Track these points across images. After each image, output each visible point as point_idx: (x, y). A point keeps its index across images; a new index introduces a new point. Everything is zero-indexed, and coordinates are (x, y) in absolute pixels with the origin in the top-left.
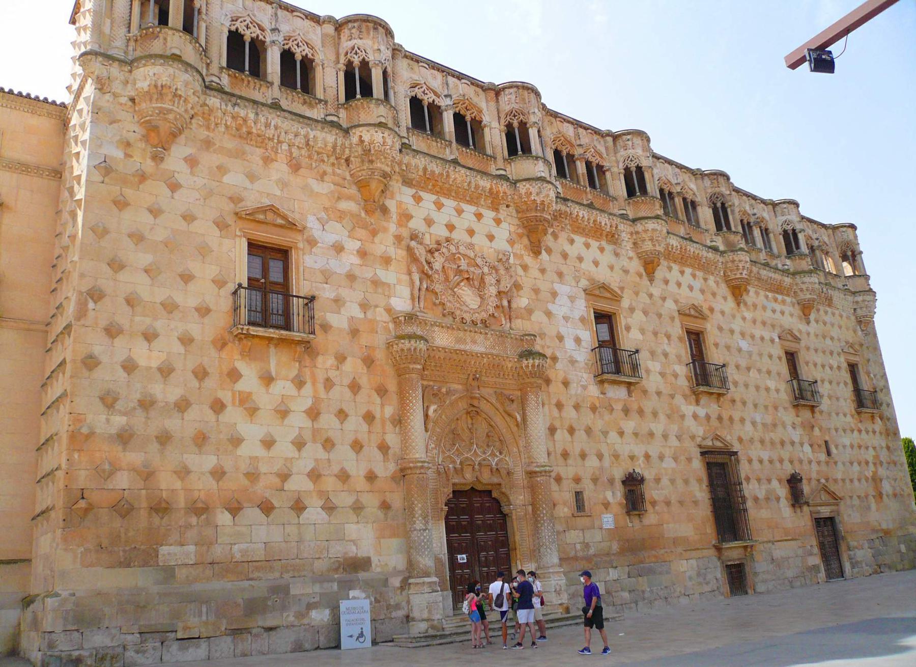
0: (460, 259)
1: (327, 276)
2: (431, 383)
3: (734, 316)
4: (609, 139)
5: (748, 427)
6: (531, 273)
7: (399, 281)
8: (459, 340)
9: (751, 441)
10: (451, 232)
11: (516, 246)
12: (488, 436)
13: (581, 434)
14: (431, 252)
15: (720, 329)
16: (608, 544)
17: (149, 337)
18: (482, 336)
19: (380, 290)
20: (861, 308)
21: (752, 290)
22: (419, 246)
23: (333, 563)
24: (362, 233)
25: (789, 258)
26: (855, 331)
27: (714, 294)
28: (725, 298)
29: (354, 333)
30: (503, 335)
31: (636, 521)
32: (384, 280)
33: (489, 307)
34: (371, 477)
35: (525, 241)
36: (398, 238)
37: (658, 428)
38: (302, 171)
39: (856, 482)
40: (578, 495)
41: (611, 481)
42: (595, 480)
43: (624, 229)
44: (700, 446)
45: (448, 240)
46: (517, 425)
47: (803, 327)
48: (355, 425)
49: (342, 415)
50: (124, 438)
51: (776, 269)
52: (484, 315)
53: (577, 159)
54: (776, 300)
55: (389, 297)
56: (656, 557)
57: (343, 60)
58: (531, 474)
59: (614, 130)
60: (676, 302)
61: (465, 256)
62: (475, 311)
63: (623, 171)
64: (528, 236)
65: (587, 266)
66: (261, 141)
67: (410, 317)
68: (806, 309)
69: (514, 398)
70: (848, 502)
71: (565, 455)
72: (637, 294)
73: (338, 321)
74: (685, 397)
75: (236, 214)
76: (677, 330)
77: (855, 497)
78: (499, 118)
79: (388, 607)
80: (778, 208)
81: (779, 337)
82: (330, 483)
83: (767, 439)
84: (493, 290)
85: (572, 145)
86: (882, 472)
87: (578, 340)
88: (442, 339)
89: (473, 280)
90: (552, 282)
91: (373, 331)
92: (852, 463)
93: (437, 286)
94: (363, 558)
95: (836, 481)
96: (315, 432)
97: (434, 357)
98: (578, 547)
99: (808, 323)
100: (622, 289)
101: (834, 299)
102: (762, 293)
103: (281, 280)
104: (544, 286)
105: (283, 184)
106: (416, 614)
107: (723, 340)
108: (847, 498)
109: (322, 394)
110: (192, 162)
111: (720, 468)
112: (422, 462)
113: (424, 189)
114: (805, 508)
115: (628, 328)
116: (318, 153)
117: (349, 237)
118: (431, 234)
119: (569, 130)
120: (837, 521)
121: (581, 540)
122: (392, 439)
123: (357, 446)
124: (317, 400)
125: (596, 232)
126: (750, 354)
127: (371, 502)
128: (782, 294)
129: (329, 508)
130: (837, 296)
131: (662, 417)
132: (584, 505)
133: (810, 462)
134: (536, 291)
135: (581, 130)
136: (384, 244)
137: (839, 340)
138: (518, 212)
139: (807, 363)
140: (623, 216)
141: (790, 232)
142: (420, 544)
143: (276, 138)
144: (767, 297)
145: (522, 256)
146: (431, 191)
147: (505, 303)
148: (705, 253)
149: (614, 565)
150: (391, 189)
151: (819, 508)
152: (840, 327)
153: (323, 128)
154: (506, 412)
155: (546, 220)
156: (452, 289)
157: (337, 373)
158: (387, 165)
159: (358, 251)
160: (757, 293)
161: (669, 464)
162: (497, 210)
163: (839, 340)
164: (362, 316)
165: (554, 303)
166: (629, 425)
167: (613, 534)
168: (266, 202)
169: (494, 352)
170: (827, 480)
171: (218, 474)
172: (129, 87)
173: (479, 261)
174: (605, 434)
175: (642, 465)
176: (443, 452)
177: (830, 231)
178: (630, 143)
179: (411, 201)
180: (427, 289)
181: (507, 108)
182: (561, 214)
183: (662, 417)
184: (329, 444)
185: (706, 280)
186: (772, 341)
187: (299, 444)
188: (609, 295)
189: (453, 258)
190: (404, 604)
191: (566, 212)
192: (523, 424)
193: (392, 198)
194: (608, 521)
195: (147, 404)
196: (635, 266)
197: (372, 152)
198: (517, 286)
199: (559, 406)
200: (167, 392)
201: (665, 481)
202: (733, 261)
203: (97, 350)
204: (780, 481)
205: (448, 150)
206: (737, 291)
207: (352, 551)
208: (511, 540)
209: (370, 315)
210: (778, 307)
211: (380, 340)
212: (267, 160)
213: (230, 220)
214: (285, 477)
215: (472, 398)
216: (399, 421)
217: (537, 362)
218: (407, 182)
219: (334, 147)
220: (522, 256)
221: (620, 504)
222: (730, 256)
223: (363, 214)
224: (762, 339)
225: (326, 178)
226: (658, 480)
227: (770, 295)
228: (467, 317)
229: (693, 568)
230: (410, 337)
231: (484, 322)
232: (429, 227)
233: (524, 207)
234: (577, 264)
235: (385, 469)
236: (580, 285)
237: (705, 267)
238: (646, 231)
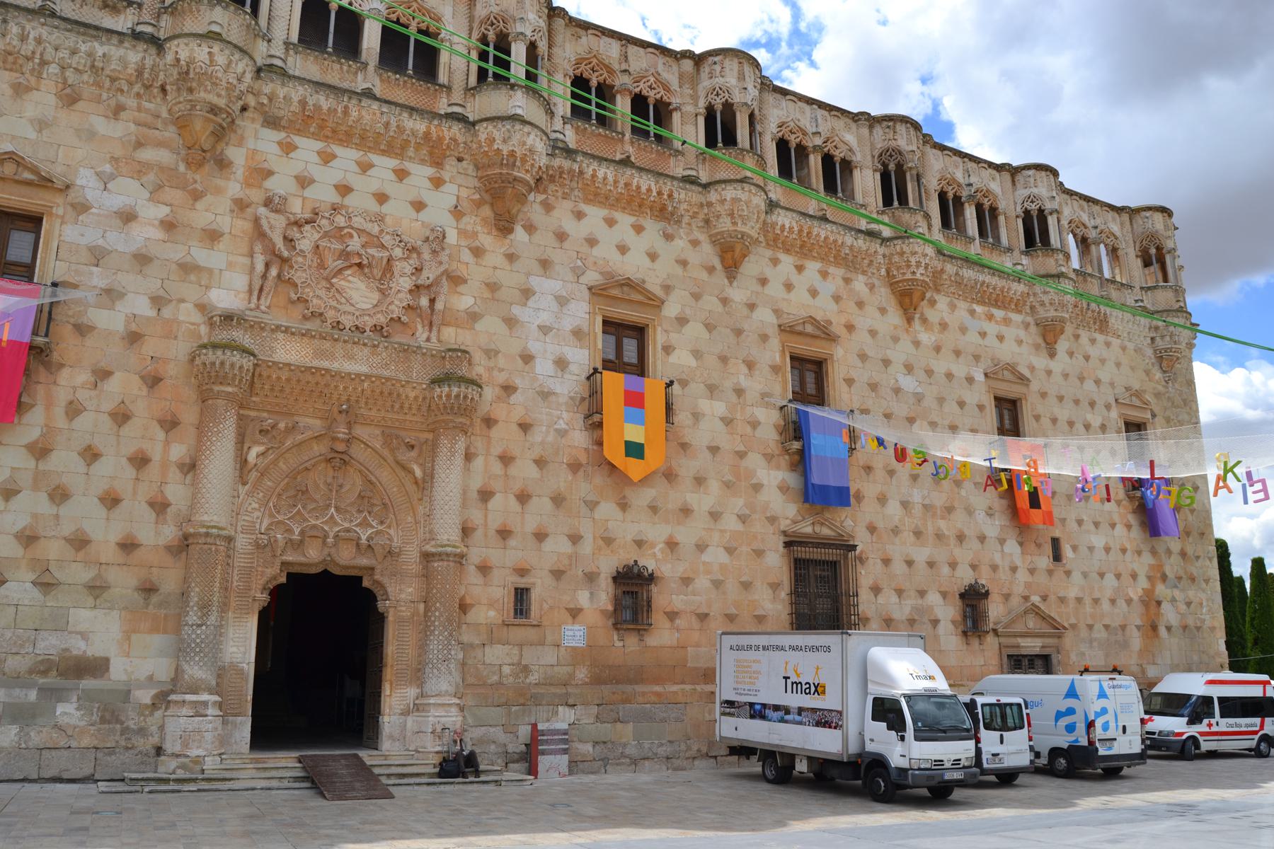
0: (351, 236)
1: (98, 256)
2: (265, 415)
3: (896, 339)
4: (688, 65)
5: (893, 508)
6: (486, 261)
7: (230, 265)
9: (896, 531)
10: (343, 196)
11: (466, 219)
12: (361, 497)
13: (541, 504)
14: (298, 224)
15: (863, 357)
16: (569, 669)
18: (366, 350)
19: (193, 277)
20: (1163, 337)
21: (942, 302)
22: (272, 215)
23: (42, 662)
24: (175, 195)
25: (1026, 253)
26: (1147, 372)
27: (860, 304)
28: (883, 311)
29: (134, 338)
30: (406, 350)
31: (632, 641)
32: (202, 264)
33: (392, 307)
34: (128, 546)
35: (487, 211)
36: (241, 205)
37: (702, 502)
38: (80, 105)
39: (1106, 605)
40: (521, 595)
41: (591, 578)
42: (558, 574)
43: (686, 197)
44: (785, 533)
45: (335, 208)
46: (416, 483)
47: (1041, 362)
48: (113, 469)
49: (91, 455)
51: (995, 271)
52: (382, 319)
53: (618, 92)
54: (990, 317)
55: (208, 287)
56: (658, 694)
58: (427, 557)
59: (698, 50)
60: (777, 312)
61: (361, 231)
62: (364, 313)
63: (703, 111)
64: (492, 205)
65: (605, 252)
68: (1049, 334)
69: (413, 442)
70: (1084, 633)
71: (504, 534)
72: (697, 297)
73: (110, 320)
74: (769, 457)
76: (774, 353)
77: (1098, 627)
78: (471, 30)
79: (125, 731)
80: (1019, 177)
81: (986, 375)
82: (53, 550)
83: (930, 530)
84: (406, 283)
85: (611, 71)
86: (1161, 590)
87: (561, 364)
88: (289, 352)
89: (370, 265)
90: (528, 274)
91: (170, 335)
92: (1102, 575)
93: (299, 273)
94: (96, 659)
95: (1062, 600)
97: (269, 377)
98: (506, 670)
99: (1052, 355)
100: (667, 288)
101: (1112, 320)
102: (962, 305)
103: (27, 259)
104: (509, 278)
105: (41, 125)
106: (169, 747)
107: (862, 375)
108: (1082, 626)
109: (61, 422)
112: (208, 527)
113: (299, 132)
114: (990, 639)
115: (668, 349)
116: (113, 80)
117: (150, 200)
118: (304, 199)
119: (612, 50)
120: (1054, 661)
121: (516, 660)
122: (176, 492)
123: (111, 501)
124: (49, 431)
125: (633, 202)
126: (919, 398)
127: (123, 581)
128: (1005, 308)
129: (46, 586)
130: (1117, 319)
131: (714, 486)
132: (528, 610)
133: (1014, 569)
135: (632, 49)
137: (1112, 384)
138: (477, 168)
139: (1037, 418)
140: (690, 181)
141: (1035, 214)
142: (189, 645)
143: (38, 56)
144: (972, 312)
145: (475, 234)
146: (315, 136)
147: (424, 302)
148: (849, 239)
149: (571, 701)
150: (239, 132)
151: (1019, 640)
152: (1118, 365)
153: (121, 42)
154: (398, 462)
155: (515, 179)
156: (327, 279)
157: (93, 393)
158: (219, 96)
159: (162, 222)
160: (953, 307)
161: (715, 555)
162: (438, 164)
163: (1112, 384)
164: (151, 313)
165: (525, 305)
168: (10, 148)
169: (386, 373)
170: (1044, 598)
173: (387, 240)
174: (592, 505)
175: (659, 555)
176: (271, 516)
177: (1126, 217)
178: (718, 68)
179: (275, 149)
180: (279, 276)
182: (561, 173)
183: (714, 486)
184: (60, 495)
185: (847, 281)
186: (970, 380)
188: (639, 297)
189: (339, 234)
190: (154, 729)
191: (571, 171)
192: (425, 485)
193: (240, 145)
194: (574, 635)
197: (191, 75)
198: (456, 280)
199: (506, 460)
201: (702, 582)
202: (902, 254)
204: (944, 595)
205: (360, 76)
206: (907, 300)
207: (79, 647)
209: (167, 312)
210: (992, 328)
211: (180, 349)
215: (334, 439)
216: (191, 467)
217: (455, 390)
218: (272, 122)
219: (140, 72)
220: (475, 235)
221: (603, 612)
223: (182, 168)
224: (949, 376)
225: (123, 115)
226: (686, 581)
227: (979, 309)
228: (347, 321)
230: (224, 347)
231: (377, 329)
232: (303, 188)
233: (485, 161)
234: (585, 249)
235: (156, 535)
236: (582, 279)
237: (850, 262)
238: (723, 201)
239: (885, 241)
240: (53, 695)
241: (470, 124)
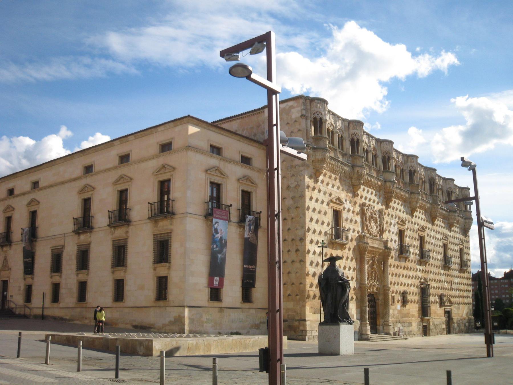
4: (406, 157)
8: (373, 243)
47: (449, 234)
57: (350, 136)
60: (418, 225)
87: (395, 241)
99: (450, 232)
111: (424, 291)
136: (358, 209)
167: (400, 312)
181: (384, 150)
208: (377, 311)
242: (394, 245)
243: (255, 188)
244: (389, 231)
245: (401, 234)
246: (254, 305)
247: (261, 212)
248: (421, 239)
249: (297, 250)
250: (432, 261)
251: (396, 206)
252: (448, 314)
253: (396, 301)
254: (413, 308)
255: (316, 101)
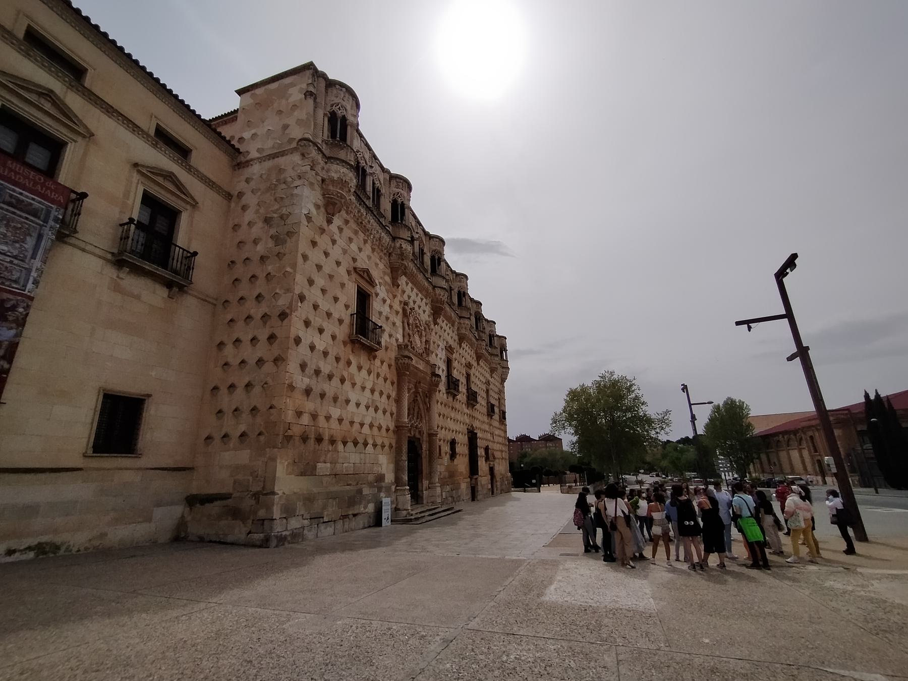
8: (416, 362)
17: (321, 331)
36: (401, 302)
49: (381, 393)
50: (308, 392)
66: (365, 230)
67: (406, 346)
75: (355, 269)
84: (424, 339)
96: (373, 400)
105: (369, 258)
106: (400, 506)
110: (341, 230)
127: (387, 444)
129: (375, 445)
134: (434, 343)
136: (397, 307)
166: (453, 415)
171: (340, 420)
172: (324, 172)
187: (367, 407)
192: (428, 409)
195: (317, 372)
196: (456, 338)
200: (326, 367)
203: (301, 334)
212: (365, 242)
213: (352, 269)
214: (362, 425)
216: (398, 401)
222: (480, 342)
229: (464, 487)
235: (392, 426)
239: (477, 340)
240: (380, 489)
241: (434, 287)
242: (442, 371)
243: (188, 207)
244: (437, 355)
245: (449, 362)
246: (142, 462)
247: (195, 254)
248: (468, 377)
249: (272, 338)
250: (478, 406)
251: (444, 325)
252: (492, 470)
253: (443, 454)
254: (462, 463)
255: (338, 87)
